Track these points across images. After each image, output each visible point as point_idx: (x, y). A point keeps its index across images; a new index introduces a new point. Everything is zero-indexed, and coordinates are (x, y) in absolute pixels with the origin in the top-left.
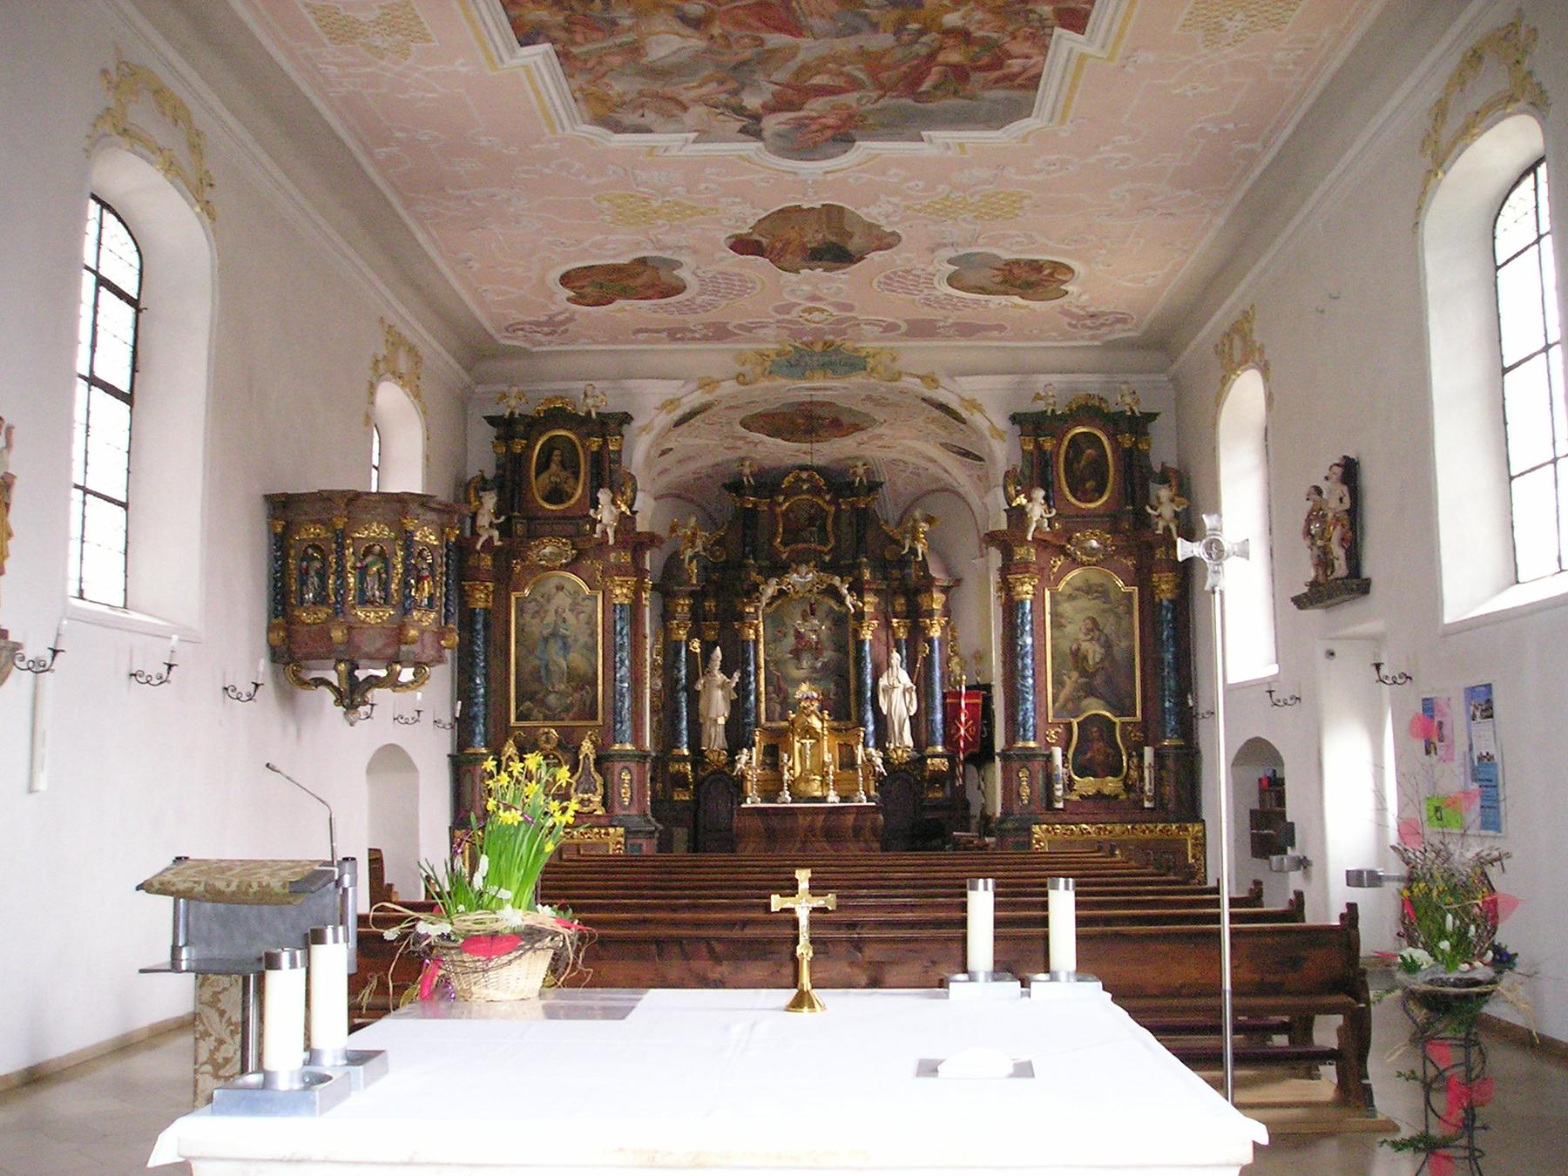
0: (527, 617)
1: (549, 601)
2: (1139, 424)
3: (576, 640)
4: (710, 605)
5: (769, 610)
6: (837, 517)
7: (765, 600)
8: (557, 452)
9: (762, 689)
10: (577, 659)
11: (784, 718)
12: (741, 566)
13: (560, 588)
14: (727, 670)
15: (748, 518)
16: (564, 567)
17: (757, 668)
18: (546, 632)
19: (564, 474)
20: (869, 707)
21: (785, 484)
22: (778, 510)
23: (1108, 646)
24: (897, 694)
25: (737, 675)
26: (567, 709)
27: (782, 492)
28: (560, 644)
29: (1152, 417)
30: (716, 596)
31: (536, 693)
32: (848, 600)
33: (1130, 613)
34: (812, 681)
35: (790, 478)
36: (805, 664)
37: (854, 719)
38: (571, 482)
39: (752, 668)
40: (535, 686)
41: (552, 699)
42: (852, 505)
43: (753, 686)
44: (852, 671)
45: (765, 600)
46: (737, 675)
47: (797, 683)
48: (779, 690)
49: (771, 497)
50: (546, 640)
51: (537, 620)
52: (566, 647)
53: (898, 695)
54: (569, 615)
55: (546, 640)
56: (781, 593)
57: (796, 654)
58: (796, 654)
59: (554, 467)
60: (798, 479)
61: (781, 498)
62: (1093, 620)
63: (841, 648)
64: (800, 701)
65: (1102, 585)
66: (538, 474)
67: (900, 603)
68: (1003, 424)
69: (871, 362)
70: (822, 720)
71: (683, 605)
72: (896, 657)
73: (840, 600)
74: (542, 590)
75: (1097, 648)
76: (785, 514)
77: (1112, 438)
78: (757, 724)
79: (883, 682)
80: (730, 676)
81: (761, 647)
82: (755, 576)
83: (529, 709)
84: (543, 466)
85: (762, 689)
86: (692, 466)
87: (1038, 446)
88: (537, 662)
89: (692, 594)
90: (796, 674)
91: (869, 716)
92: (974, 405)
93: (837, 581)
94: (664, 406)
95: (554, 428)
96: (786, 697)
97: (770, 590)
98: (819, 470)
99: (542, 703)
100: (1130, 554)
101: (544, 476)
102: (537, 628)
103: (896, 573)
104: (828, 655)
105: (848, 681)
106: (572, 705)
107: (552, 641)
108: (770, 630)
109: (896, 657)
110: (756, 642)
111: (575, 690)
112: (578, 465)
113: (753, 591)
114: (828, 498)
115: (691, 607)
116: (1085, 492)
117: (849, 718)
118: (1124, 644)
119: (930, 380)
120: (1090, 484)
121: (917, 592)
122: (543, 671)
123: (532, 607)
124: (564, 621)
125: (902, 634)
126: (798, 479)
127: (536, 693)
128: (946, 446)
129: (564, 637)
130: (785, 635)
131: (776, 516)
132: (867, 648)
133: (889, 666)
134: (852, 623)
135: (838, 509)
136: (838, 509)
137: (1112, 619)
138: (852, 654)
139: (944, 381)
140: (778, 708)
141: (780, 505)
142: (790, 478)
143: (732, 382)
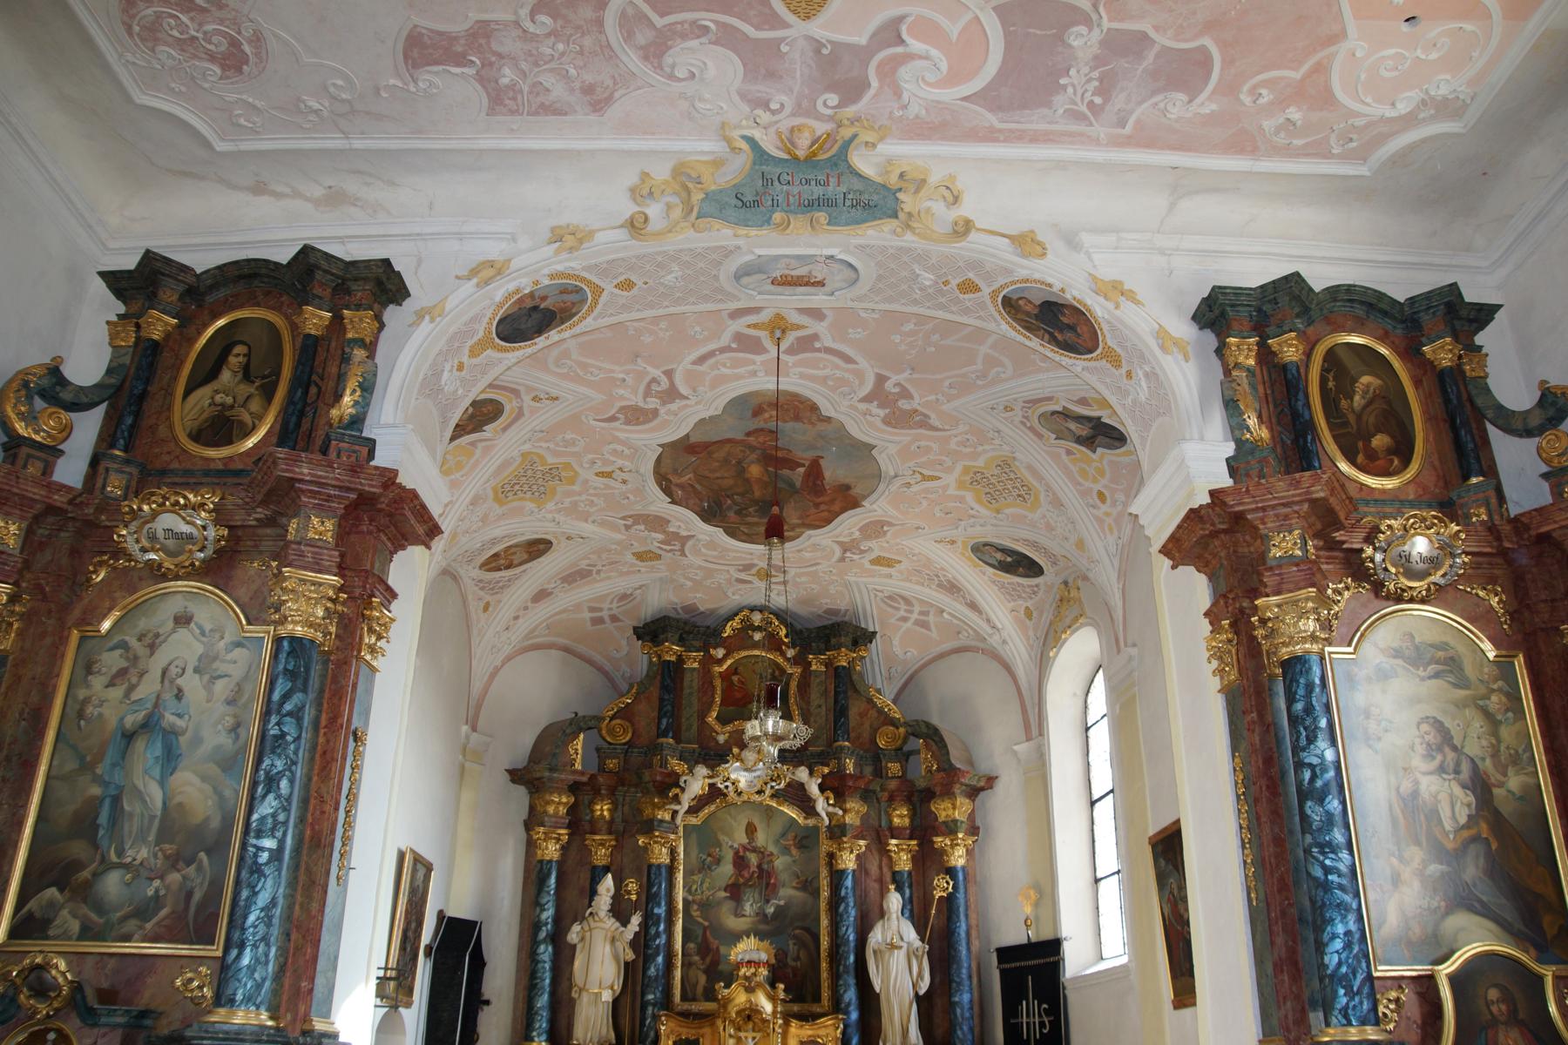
0: (97, 682)
1: (152, 647)
2: (1461, 316)
3: (197, 741)
4: (603, 809)
5: (693, 821)
6: (804, 686)
7: (686, 801)
8: (239, 349)
9: (678, 946)
10: (194, 789)
11: (710, 995)
12: (654, 748)
13: (183, 620)
14: (620, 912)
15: (670, 674)
16: (195, 573)
17: (671, 911)
18: (130, 721)
19: (245, 389)
20: (852, 981)
21: (728, 631)
22: (717, 669)
23: (1481, 787)
24: (898, 960)
25: (636, 920)
26: (143, 912)
27: (723, 643)
28: (158, 749)
29: (1484, 314)
30: (612, 792)
31: (77, 865)
32: (821, 806)
33: (1520, 713)
34: (761, 936)
35: (736, 623)
36: (748, 908)
37: (825, 994)
38: (255, 405)
39: (661, 910)
40: (78, 849)
41: (113, 885)
42: (828, 664)
43: (662, 940)
44: (824, 922)
45: (686, 801)
46: (636, 920)
47: (736, 937)
48: (705, 949)
49: (705, 648)
50: (129, 737)
51: (117, 693)
52: (170, 759)
53: (898, 963)
54: (191, 684)
55: (129, 737)
56: (714, 793)
57: (735, 892)
58: (735, 892)
59: (226, 376)
60: (748, 626)
61: (720, 653)
62: (1438, 725)
63: (808, 886)
64: (738, 965)
65: (1443, 646)
66: (188, 392)
67: (901, 816)
68: (1183, 329)
69: (907, 201)
70: (772, 999)
71: (558, 804)
72: (894, 901)
73: (807, 805)
74: (142, 624)
75: (1458, 791)
76: (725, 676)
77: (1411, 352)
78: (666, 1003)
79: (876, 937)
80: (625, 922)
81: (680, 877)
82: (676, 765)
83: (51, 904)
84: (208, 372)
85: (678, 946)
86: (585, 593)
87: (1266, 355)
88: (96, 791)
89: (574, 788)
90: (733, 923)
91: (850, 995)
92: (1116, 290)
93: (802, 774)
94: (474, 272)
95: (241, 307)
96: (716, 962)
97: (697, 784)
98: (781, 615)
99: (84, 893)
100: (1493, 580)
101: (203, 394)
102: (111, 706)
103: (894, 768)
104: (788, 893)
105: (816, 938)
106: (157, 900)
107: (140, 744)
108: (694, 853)
109: (894, 901)
110: (671, 869)
111: (174, 862)
112: (277, 373)
113: (669, 786)
114: (790, 653)
115: (573, 810)
116: (1372, 455)
117: (817, 998)
118: (1515, 782)
119: (1026, 243)
120: (1380, 441)
121: (929, 795)
122: (103, 819)
123: (112, 660)
124: (179, 695)
125: (904, 863)
126: (748, 626)
127: (77, 865)
128: (981, 550)
129: (170, 735)
130: (718, 861)
131: (712, 677)
132: (849, 882)
133: (882, 914)
134: (825, 846)
135: (807, 674)
136: (807, 674)
137: (1478, 725)
138: (825, 894)
139: (1055, 245)
140: (703, 979)
141: (720, 662)
142: (736, 623)
143: (622, 234)
